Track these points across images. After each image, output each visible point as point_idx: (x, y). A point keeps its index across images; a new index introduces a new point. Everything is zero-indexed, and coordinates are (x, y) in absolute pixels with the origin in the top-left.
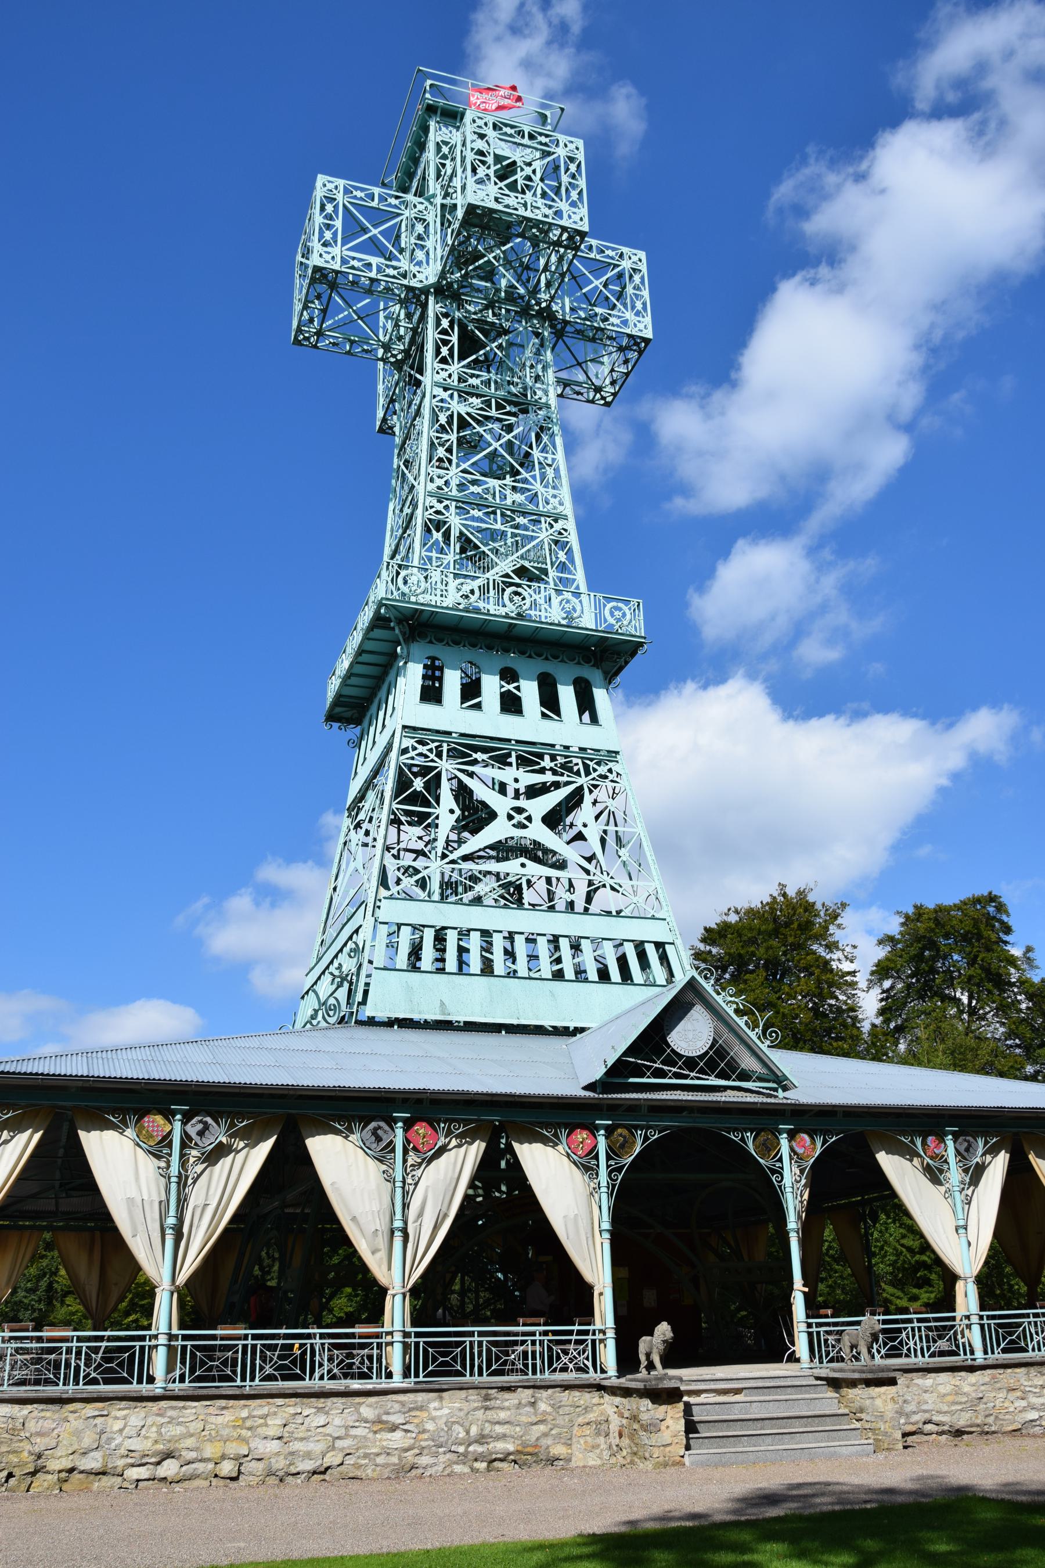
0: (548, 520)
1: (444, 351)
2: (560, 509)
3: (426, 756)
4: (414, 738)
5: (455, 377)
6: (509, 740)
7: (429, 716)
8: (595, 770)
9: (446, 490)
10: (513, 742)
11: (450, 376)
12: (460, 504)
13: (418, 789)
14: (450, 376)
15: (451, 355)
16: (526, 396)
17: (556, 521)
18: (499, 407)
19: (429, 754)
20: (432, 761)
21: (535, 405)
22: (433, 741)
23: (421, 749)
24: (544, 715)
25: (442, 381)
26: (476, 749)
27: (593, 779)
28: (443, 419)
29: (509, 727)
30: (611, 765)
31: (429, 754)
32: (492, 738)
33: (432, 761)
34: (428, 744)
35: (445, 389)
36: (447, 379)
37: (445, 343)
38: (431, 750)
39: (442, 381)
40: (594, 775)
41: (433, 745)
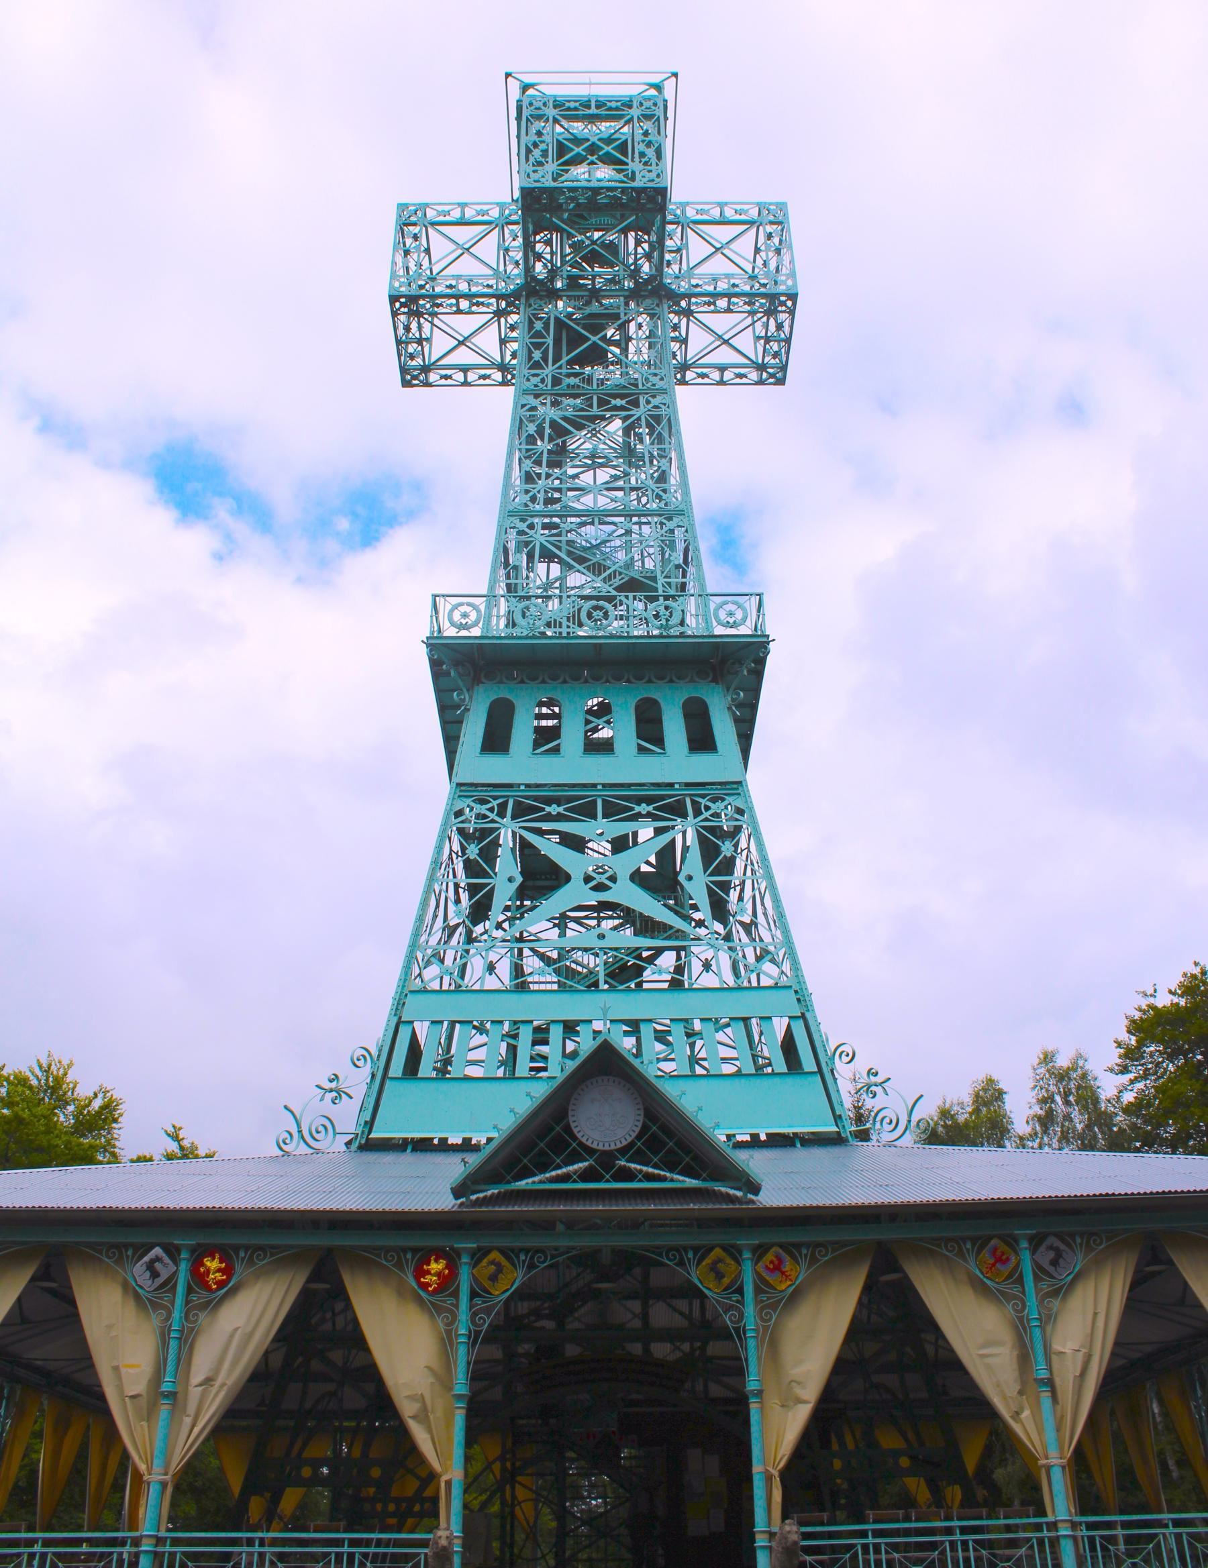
1: (537, 355)
3: (485, 817)
4: (472, 796)
5: (549, 381)
6: (594, 786)
7: (495, 769)
8: (707, 808)
10: (600, 787)
11: (543, 381)
13: (472, 857)
14: (543, 381)
15: (545, 359)
16: (636, 386)
17: (670, 519)
18: (602, 403)
19: (488, 813)
20: (493, 821)
21: (647, 394)
22: (495, 798)
23: (483, 809)
24: (641, 750)
25: (533, 387)
26: (549, 801)
27: (706, 820)
28: (531, 428)
29: (599, 770)
30: (729, 799)
31: (488, 813)
32: (574, 786)
33: (493, 821)
34: (490, 802)
35: (537, 396)
36: (540, 384)
37: (537, 346)
38: (491, 810)
39: (533, 387)
40: (706, 814)
41: (495, 803)
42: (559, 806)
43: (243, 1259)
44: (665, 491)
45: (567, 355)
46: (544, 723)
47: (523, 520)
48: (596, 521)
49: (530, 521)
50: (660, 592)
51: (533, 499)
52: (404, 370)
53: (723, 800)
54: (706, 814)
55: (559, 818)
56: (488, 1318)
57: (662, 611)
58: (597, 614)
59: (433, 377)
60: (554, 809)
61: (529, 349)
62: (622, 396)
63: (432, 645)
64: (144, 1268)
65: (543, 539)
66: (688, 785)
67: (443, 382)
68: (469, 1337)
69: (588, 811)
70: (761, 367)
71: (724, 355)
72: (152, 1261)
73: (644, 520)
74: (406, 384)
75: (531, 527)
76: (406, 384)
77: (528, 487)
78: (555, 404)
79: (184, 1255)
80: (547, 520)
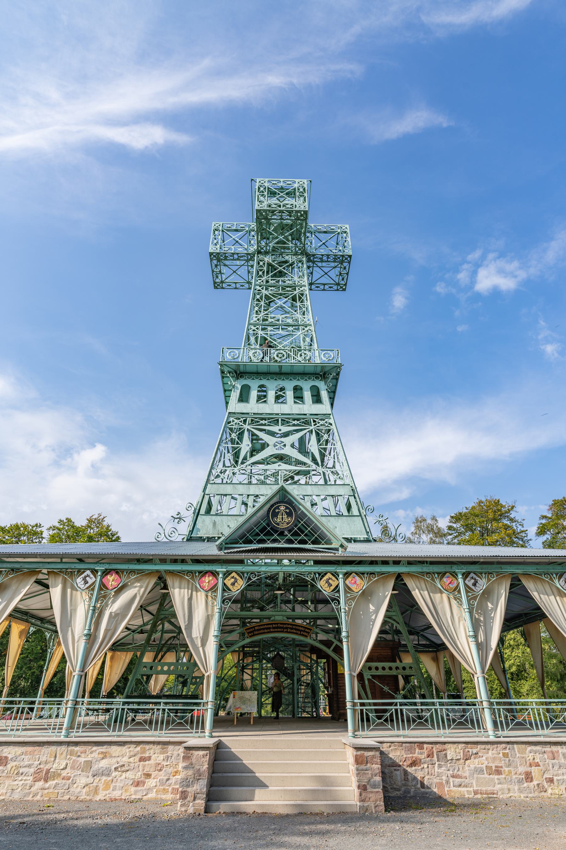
0: (302, 327)
2: (308, 322)
9: (258, 322)
12: (263, 327)
17: (306, 327)
42: (265, 421)
43: (125, 576)
44: (304, 318)
45: (272, 272)
46: (261, 393)
47: (255, 326)
48: (280, 327)
49: (258, 326)
50: (302, 348)
51: (258, 320)
52: (215, 283)
53: (324, 420)
54: (318, 425)
55: (265, 425)
56: (230, 601)
57: (303, 354)
58: (280, 355)
59: (224, 285)
60: (263, 422)
61: (258, 271)
62: (290, 287)
63: (221, 364)
64: (82, 579)
65: (262, 333)
66: (311, 414)
67: (228, 287)
68: (221, 610)
69: (276, 422)
70: (338, 284)
71: (325, 280)
72: (85, 577)
73: (297, 327)
74: (216, 288)
75: (257, 328)
76: (216, 288)
77: (257, 316)
78: (266, 289)
79: (99, 573)
80: (263, 327)
